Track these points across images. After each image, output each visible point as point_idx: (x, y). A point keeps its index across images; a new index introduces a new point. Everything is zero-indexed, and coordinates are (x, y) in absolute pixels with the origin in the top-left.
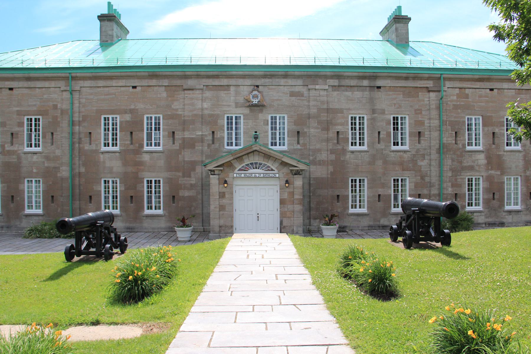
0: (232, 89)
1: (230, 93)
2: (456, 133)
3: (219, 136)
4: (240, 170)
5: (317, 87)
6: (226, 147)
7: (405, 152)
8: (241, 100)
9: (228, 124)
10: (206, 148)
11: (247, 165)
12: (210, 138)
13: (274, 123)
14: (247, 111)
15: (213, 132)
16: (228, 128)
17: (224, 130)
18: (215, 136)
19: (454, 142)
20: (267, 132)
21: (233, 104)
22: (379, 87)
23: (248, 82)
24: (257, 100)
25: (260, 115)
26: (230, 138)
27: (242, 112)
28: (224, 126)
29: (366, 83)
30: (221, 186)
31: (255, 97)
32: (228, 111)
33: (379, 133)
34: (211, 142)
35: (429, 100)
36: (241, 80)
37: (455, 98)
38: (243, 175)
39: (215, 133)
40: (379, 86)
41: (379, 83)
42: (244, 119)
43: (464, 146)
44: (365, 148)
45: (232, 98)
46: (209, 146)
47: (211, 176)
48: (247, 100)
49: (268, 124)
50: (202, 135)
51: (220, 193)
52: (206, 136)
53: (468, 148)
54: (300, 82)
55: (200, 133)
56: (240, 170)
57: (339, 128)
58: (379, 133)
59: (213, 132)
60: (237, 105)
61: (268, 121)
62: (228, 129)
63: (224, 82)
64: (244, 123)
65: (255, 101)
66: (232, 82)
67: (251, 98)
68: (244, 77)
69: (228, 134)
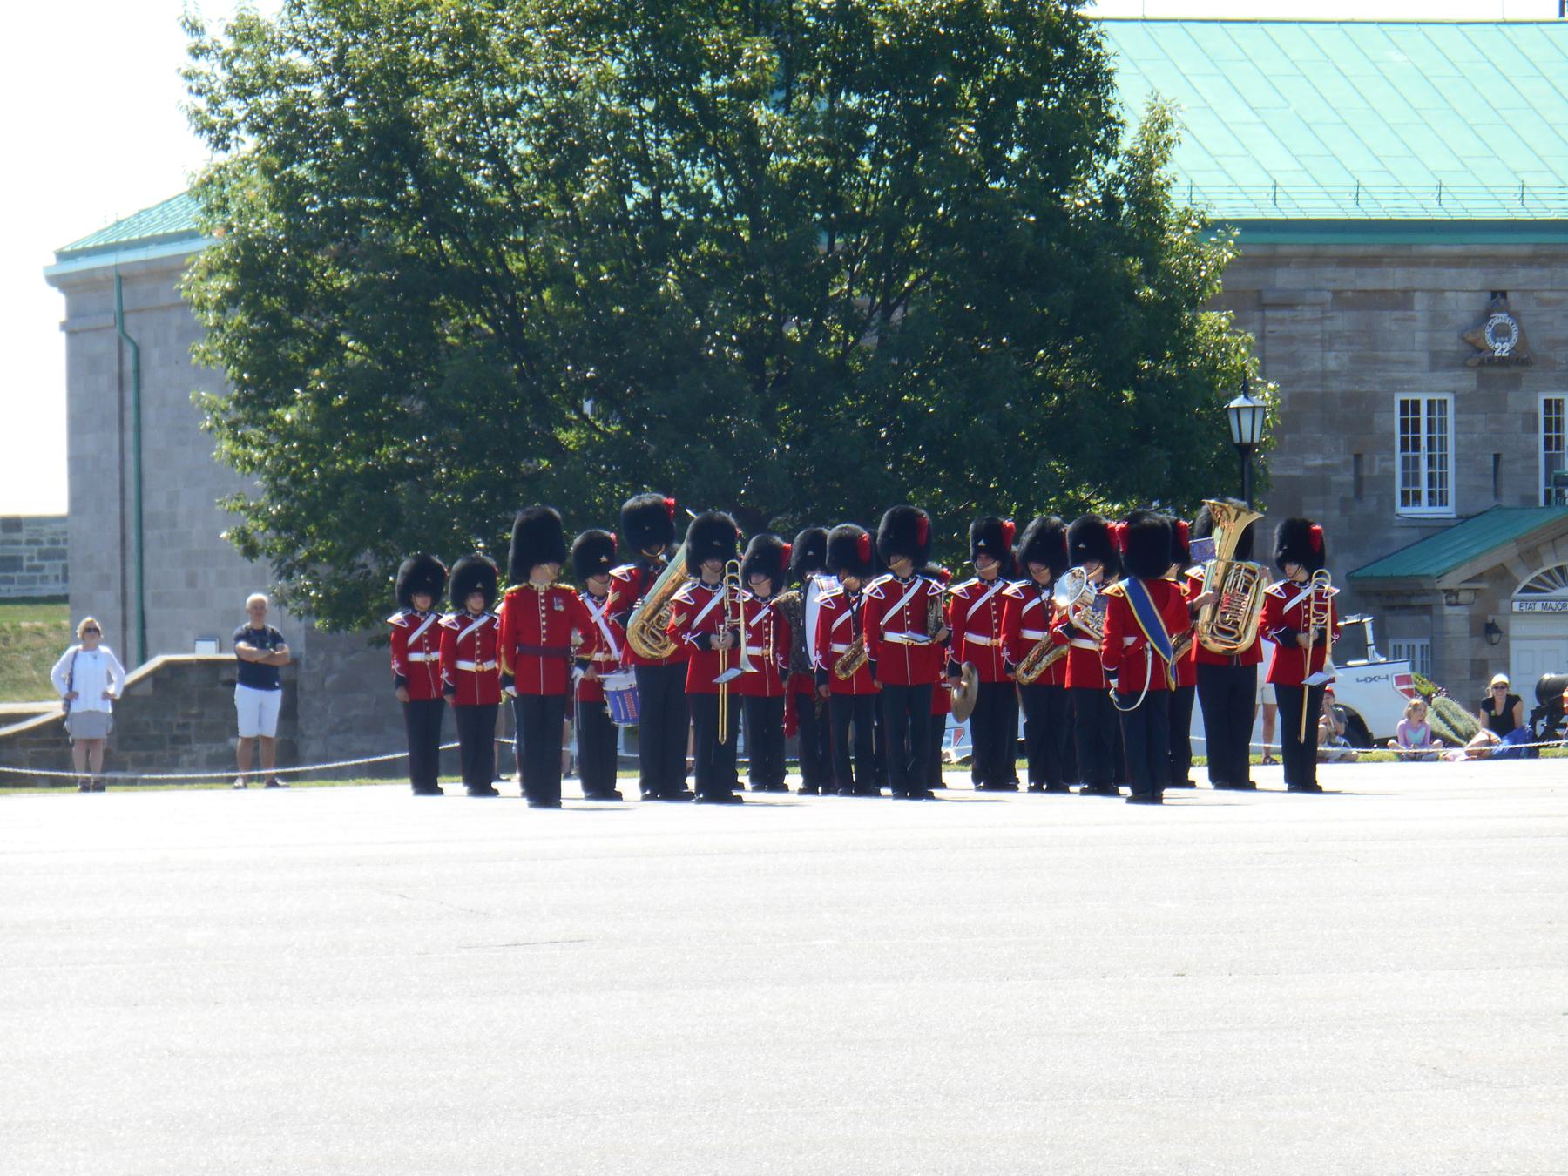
0: (1420, 302)
1: (1412, 319)
3: (1376, 472)
4: (1527, 589)
6: (1400, 510)
8: (1450, 342)
9: (1404, 429)
10: (1336, 513)
11: (1548, 573)
12: (1347, 477)
13: (1554, 425)
14: (1467, 381)
15: (1358, 457)
16: (1404, 442)
17: (1392, 449)
18: (1365, 473)
20: (1535, 455)
21: (1424, 358)
23: (1475, 278)
24: (1507, 346)
25: (1512, 396)
26: (1411, 477)
27: (1452, 386)
28: (1392, 435)
30: (1476, 640)
31: (1501, 333)
32: (1409, 381)
34: (1351, 494)
36: (1453, 271)
38: (1538, 607)
39: (1366, 458)
42: (1457, 411)
45: (1420, 337)
46: (1345, 505)
47: (1448, 610)
48: (1472, 344)
49: (1536, 430)
50: (1325, 467)
51: (1473, 661)
52: (1332, 469)
55: (1319, 462)
56: (1527, 589)
59: (1358, 457)
60: (1437, 361)
61: (1536, 416)
62: (1404, 448)
63: (1396, 278)
64: (1457, 423)
65: (1502, 349)
66: (1423, 277)
67: (1488, 336)
68: (1459, 262)
69: (1405, 460)
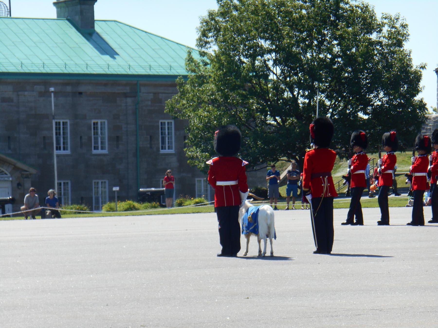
2: (151, 137)
5: (26, 93)
7: (104, 155)
19: (149, 146)
22: (80, 93)
29: (69, 89)
33: (81, 137)
35: (126, 106)
37: (149, 103)
40: (80, 91)
41: (82, 89)
43: (158, 150)
44: (68, 152)
53: (162, 151)
54: (10, 88)
57: (45, 133)
58: (81, 137)
